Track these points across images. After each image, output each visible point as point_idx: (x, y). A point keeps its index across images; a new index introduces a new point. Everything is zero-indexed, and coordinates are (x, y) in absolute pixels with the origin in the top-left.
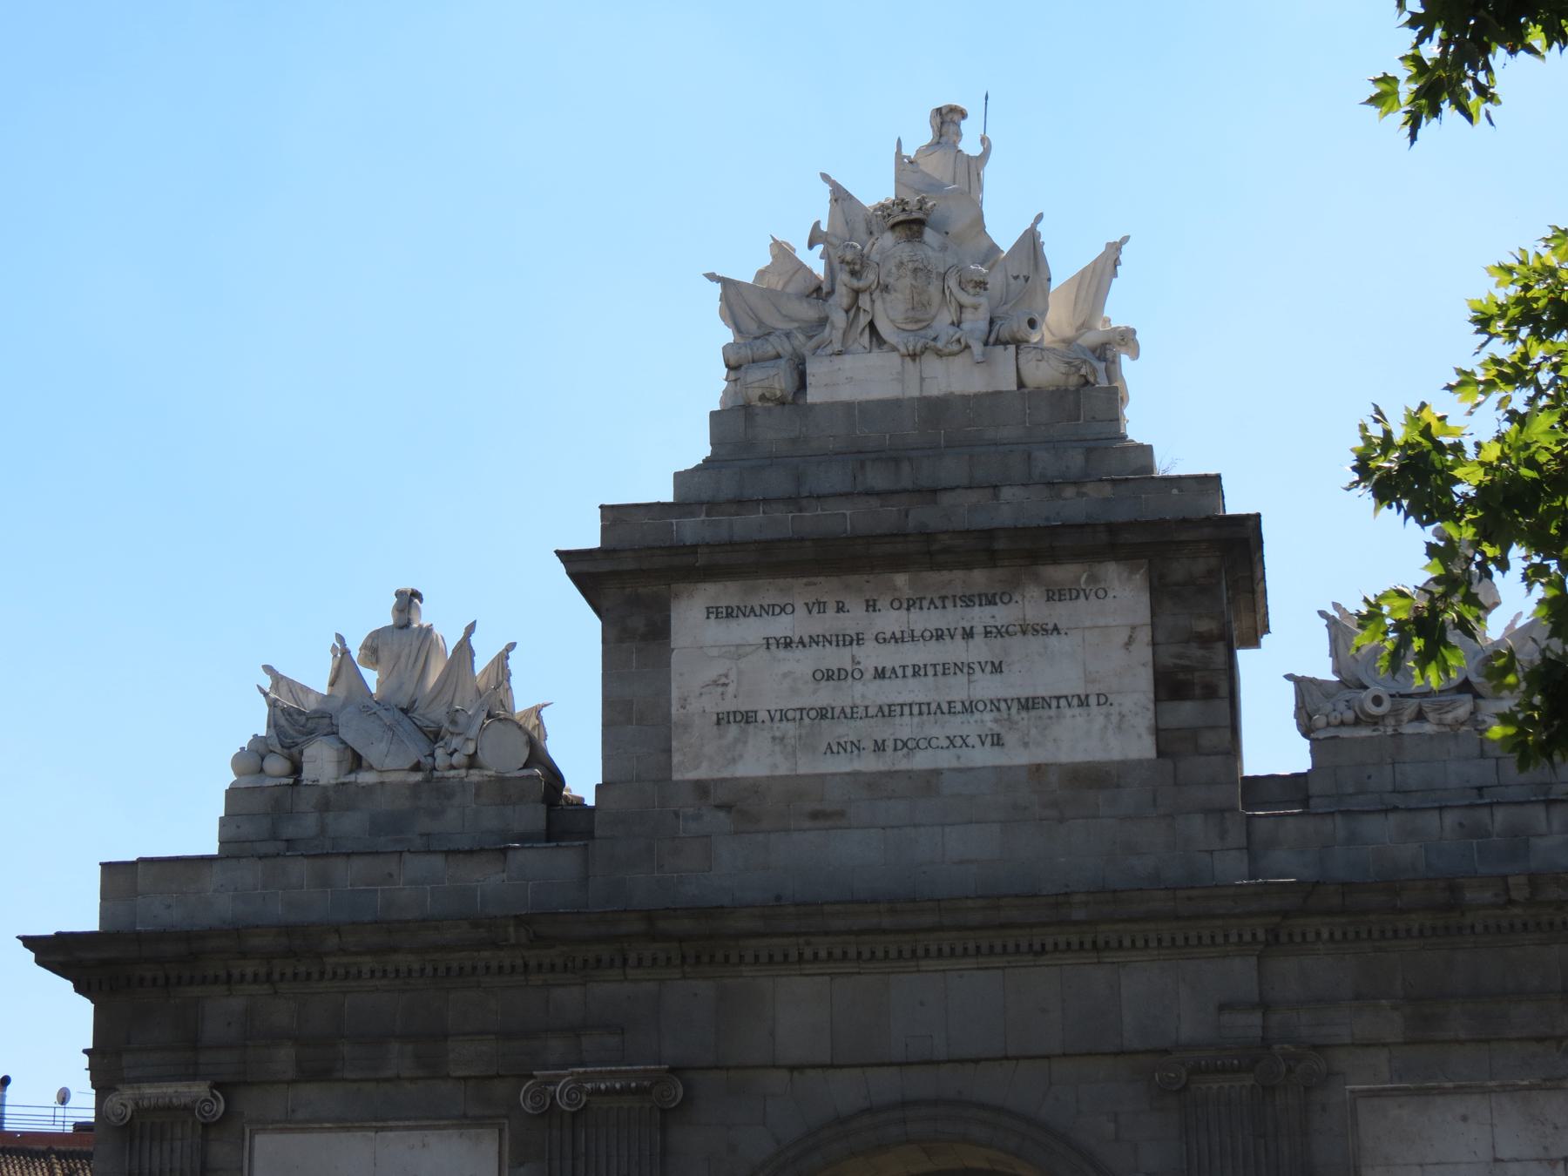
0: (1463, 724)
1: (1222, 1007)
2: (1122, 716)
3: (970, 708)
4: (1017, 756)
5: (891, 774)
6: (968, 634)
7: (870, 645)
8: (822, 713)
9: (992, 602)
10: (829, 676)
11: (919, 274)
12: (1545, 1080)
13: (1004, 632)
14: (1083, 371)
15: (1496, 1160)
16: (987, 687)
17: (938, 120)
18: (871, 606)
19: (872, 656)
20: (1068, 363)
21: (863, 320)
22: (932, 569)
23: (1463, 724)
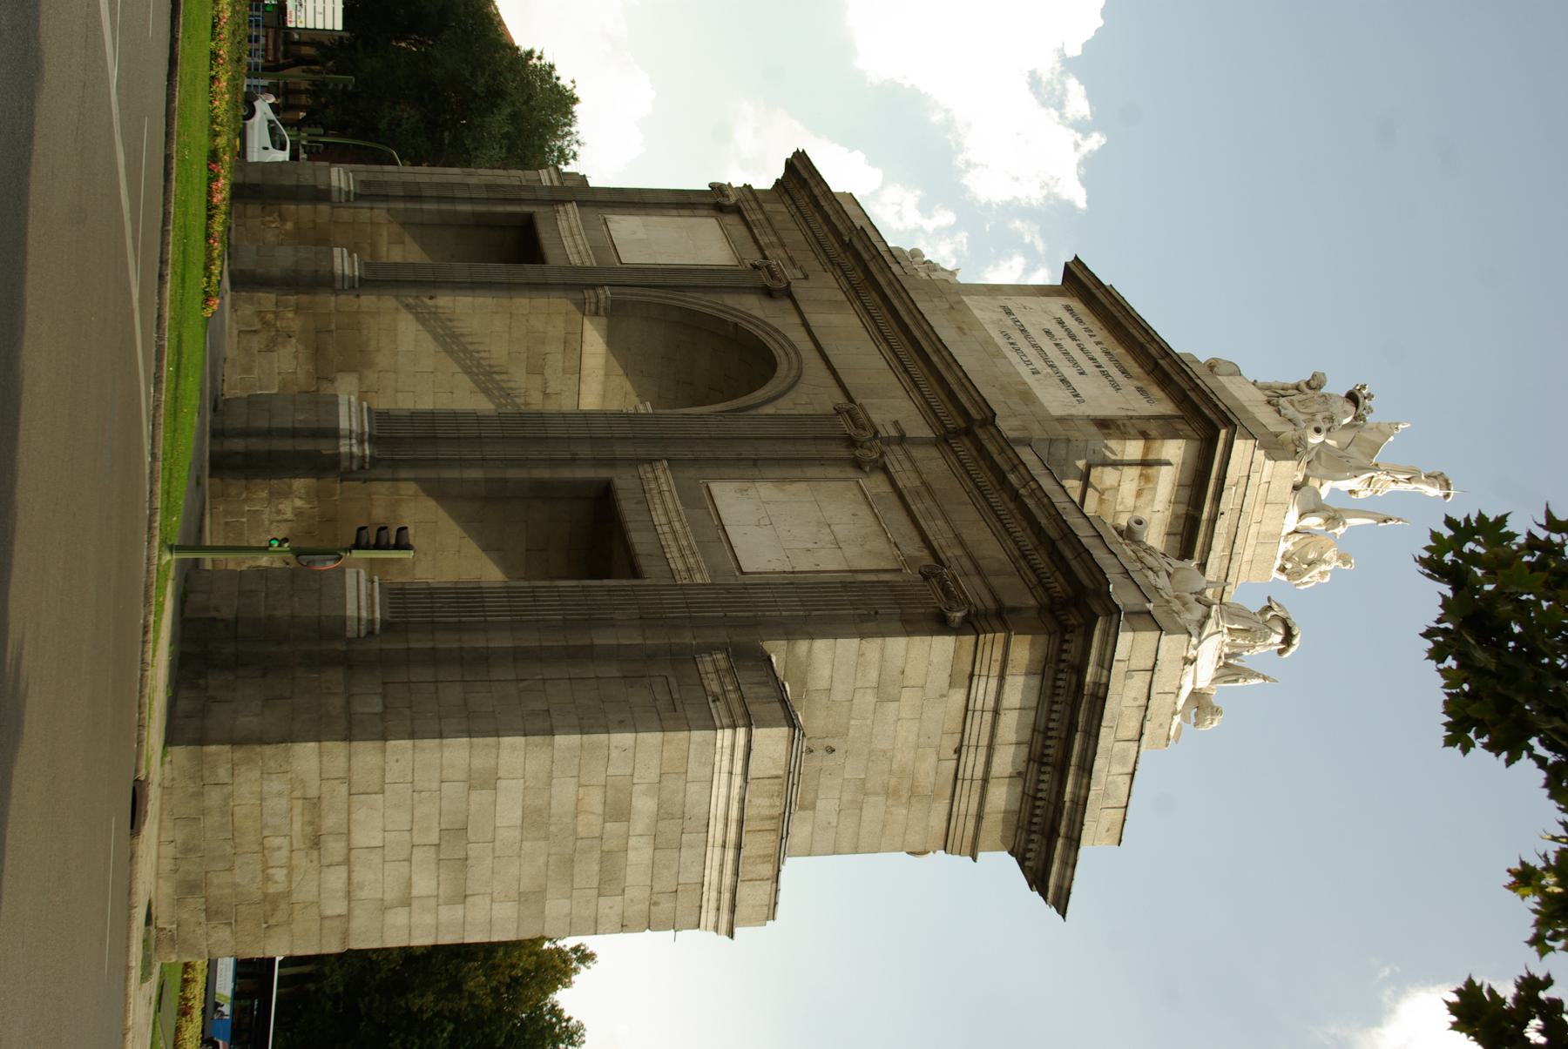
0: (1142, 562)
1: (896, 424)
2: (1074, 406)
3: (1052, 366)
4: (1030, 380)
5: (996, 345)
6: (1098, 367)
7: (1075, 343)
8: (1023, 331)
9: (1123, 373)
10: (1048, 332)
11: (1323, 398)
12: (895, 543)
13: (1105, 374)
14: (1299, 449)
15: (829, 525)
16: (1069, 372)
17: (1436, 474)
18: (1098, 343)
19: (1068, 344)
20: (1300, 438)
21: (1282, 392)
22: (1134, 359)
23: (1142, 562)
